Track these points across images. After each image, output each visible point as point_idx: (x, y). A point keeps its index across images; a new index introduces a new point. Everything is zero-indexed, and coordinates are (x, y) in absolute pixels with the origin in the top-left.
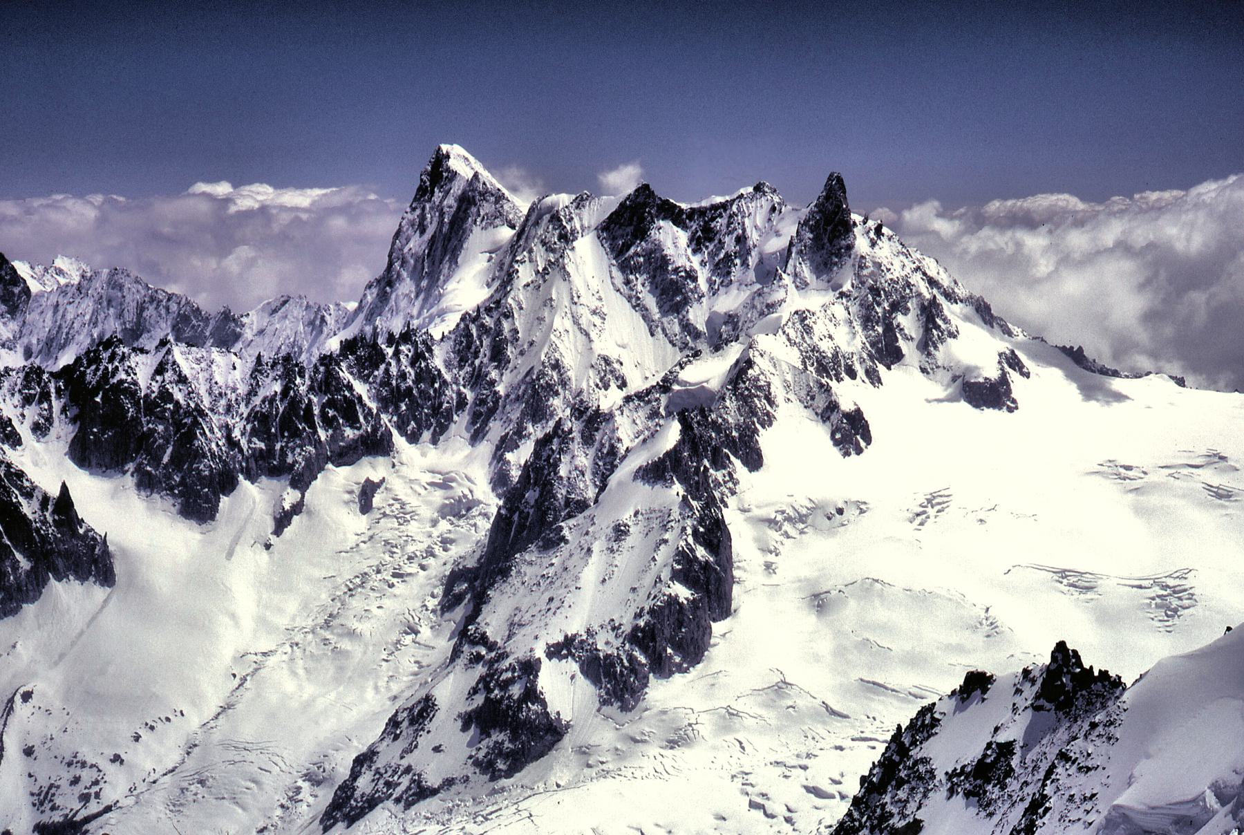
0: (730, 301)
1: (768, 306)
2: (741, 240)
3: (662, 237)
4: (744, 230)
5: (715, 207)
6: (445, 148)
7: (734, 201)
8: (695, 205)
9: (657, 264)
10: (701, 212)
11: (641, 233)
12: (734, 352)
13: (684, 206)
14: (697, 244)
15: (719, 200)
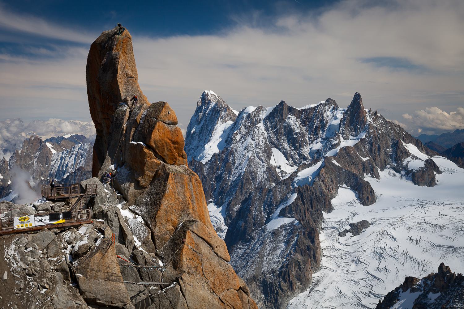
0: (317, 146)
1: (332, 145)
2: (322, 121)
3: (290, 121)
4: (323, 117)
5: (310, 109)
6: (206, 92)
7: (318, 106)
8: (303, 108)
9: (289, 132)
10: (305, 111)
11: (282, 120)
12: (319, 164)
13: (299, 109)
14: (303, 123)
15: (312, 106)
